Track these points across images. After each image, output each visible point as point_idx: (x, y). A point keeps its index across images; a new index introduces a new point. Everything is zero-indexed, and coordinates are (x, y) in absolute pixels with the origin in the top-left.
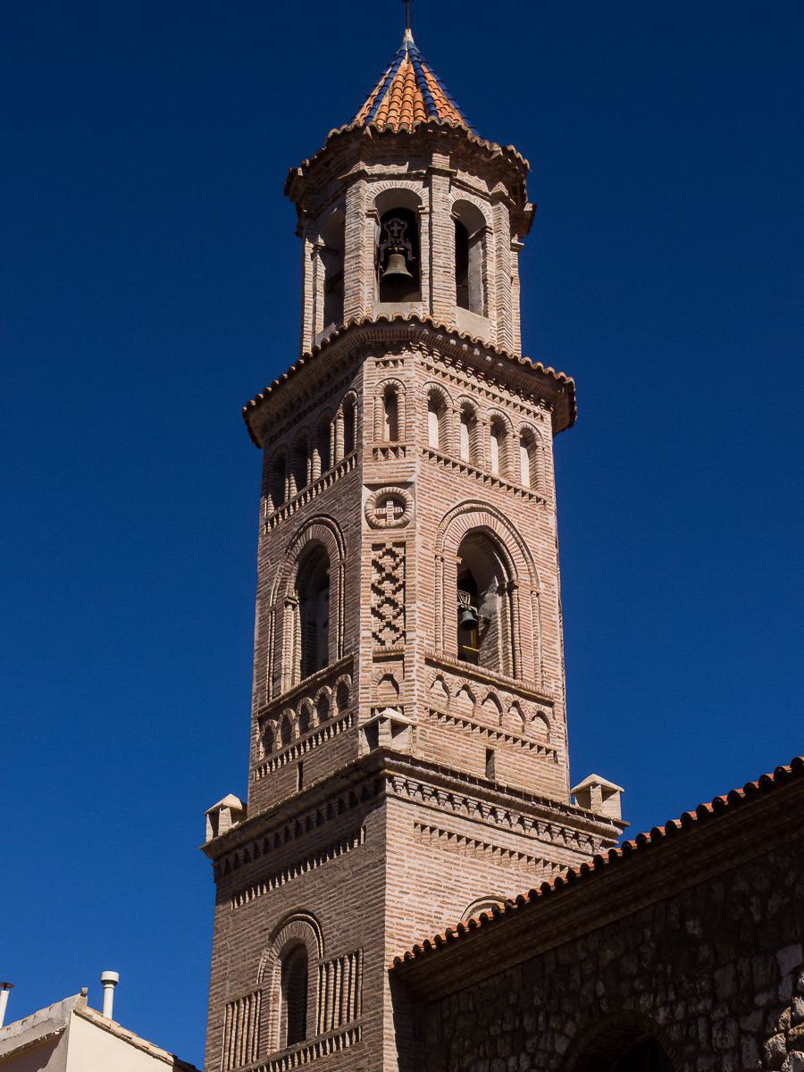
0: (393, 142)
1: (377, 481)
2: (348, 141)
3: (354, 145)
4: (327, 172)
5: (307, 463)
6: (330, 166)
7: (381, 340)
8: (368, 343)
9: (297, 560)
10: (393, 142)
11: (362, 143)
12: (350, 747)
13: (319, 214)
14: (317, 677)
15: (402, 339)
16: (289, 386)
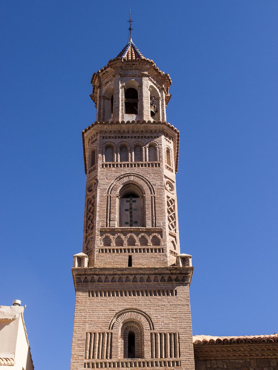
0: (156, 73)
1: (167, 175)
2: (147, 64)
3: (148, 66)
4: (131, 66)
5: (128, 155)
6: (133, 66)
7: (151, 129)
8: (165, 131)
9: (123, 184)
10: (156, 73)
11: (150, 67)
12: (162, 260)
13: (124, 77)
14: (141, 229)
15: (172, 136)
16: (123, 126)
